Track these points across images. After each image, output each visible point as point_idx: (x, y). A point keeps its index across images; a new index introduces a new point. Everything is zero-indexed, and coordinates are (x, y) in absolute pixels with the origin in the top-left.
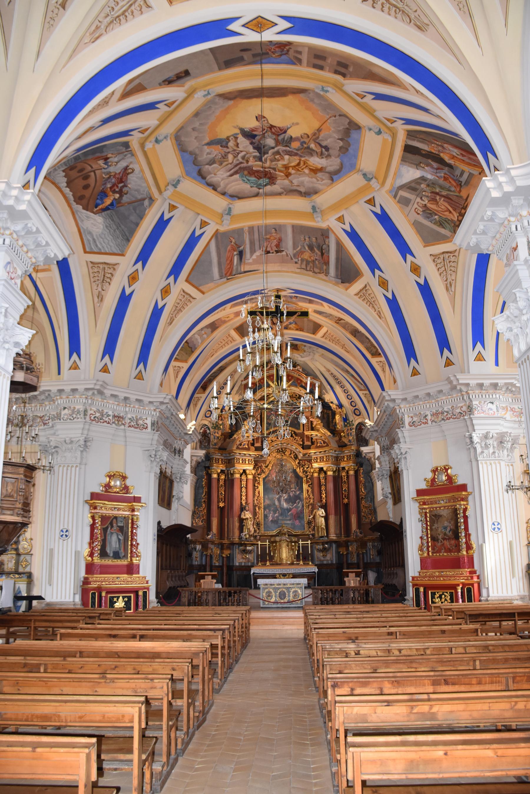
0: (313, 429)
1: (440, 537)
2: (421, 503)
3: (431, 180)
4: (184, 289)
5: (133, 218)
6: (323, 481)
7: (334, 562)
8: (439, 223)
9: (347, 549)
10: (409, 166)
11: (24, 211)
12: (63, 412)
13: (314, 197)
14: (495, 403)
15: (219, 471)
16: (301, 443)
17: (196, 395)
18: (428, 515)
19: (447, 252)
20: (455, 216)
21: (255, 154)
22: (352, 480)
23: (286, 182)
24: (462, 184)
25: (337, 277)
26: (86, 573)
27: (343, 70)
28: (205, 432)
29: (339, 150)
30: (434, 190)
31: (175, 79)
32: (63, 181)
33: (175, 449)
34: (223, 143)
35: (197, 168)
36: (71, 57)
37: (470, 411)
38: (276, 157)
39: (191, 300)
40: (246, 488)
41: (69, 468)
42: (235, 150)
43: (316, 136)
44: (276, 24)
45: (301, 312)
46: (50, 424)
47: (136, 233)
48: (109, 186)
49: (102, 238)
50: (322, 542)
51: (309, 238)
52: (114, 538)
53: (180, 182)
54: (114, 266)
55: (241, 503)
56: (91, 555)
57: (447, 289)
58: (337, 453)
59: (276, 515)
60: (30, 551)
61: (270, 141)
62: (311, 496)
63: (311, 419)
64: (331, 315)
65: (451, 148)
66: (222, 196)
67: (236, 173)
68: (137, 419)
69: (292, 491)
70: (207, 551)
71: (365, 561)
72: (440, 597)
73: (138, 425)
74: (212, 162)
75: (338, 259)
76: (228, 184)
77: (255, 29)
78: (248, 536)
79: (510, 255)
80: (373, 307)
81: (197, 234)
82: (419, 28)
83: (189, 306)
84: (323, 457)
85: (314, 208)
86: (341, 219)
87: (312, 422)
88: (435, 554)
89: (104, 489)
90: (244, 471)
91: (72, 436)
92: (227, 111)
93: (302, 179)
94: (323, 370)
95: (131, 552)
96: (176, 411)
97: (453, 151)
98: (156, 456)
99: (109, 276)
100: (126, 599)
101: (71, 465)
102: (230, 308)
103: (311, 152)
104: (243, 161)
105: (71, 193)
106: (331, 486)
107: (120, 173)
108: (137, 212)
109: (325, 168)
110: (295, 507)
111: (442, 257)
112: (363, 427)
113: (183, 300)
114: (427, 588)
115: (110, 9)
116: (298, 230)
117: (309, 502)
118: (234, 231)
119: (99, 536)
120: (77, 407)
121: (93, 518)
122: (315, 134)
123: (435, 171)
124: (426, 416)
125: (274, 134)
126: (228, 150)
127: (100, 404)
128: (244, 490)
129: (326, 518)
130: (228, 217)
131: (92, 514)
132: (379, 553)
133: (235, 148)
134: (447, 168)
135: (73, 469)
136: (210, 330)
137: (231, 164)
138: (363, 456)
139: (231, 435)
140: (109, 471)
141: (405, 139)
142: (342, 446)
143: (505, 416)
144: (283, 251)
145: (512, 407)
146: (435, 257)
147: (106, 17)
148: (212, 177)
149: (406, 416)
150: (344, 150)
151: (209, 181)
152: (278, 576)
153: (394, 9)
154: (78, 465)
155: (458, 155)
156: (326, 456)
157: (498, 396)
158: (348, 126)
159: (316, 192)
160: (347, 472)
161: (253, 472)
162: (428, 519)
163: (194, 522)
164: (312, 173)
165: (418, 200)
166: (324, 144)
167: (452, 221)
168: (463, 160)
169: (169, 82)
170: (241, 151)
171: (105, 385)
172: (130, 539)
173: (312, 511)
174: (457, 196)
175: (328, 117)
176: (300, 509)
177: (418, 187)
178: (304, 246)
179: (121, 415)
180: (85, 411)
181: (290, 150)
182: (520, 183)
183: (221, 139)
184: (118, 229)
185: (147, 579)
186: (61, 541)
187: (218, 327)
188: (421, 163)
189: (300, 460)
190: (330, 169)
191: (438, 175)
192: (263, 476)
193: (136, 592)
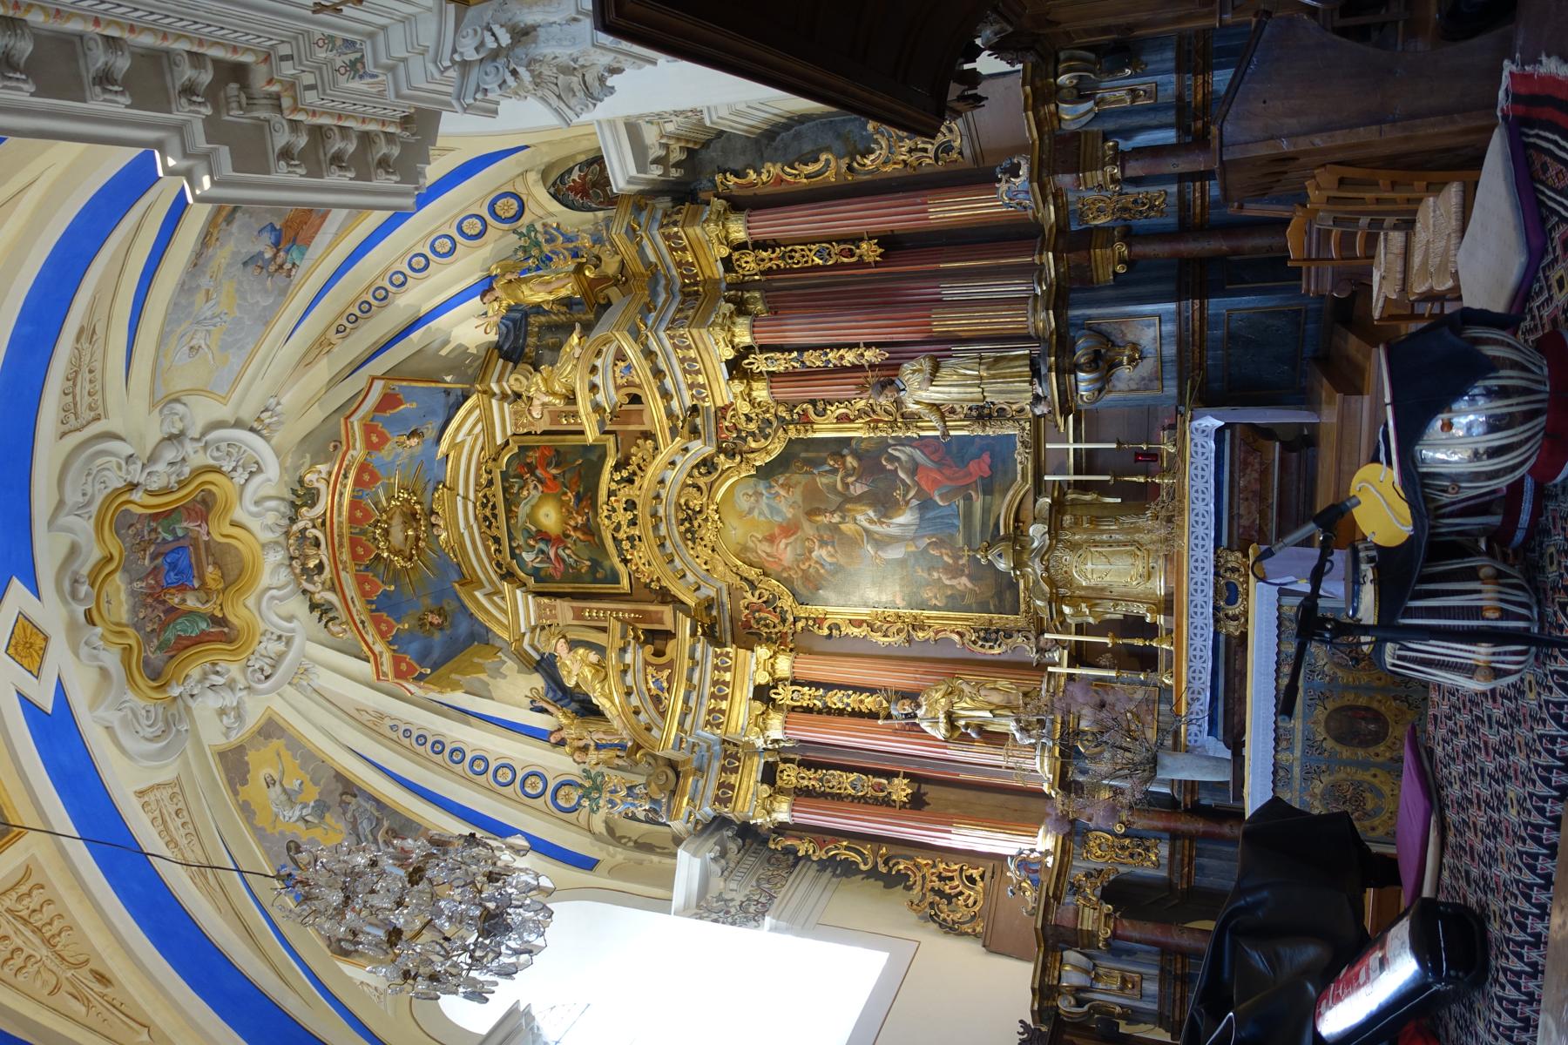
7: (1172, 306)
15: (765, 790)
22: (772, 225)
40: (829, 687)
50: (1060, 372)
59: (946, 558)
69: (846, 486)
71: (1169, 136)
84: (682, 360)
90: (762, 694)
94: (323, 370)
112: (575, 175)
128: (836, 699)
138: (675, 173)
152: (1232, 628)
160: (741, 246)
176: (918, 454)
189: (720, 450)
192: (787, 602)
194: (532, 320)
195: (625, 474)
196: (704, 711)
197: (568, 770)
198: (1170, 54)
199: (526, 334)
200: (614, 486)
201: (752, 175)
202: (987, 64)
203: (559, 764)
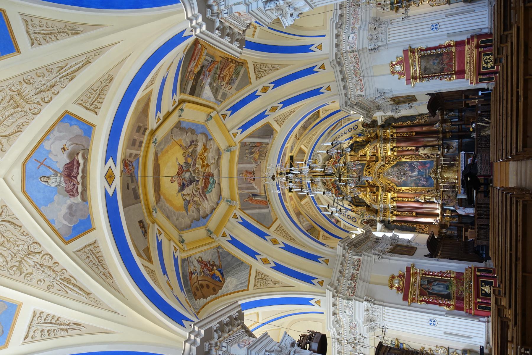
0: (365, 155)
1: (441, 66)
2: (416, 81)
3: (211, 80)
4: (274, 230)
5: (229, 259)
6: (400, 149)
7: (458, 141)
8: (237, 75)
9: (448, 132)
10: (203, 93)
11: (205, 331)
12: (348, 313)
13: (221, 150)
14: (348, 35)
16: (374, 162)
17: (342, 227)
18: (424, 76)
19: (255, 70)
20: (233, 65)
21: (194, 185)
23: (212, 166)
24: (213, 60)
25: (269, 138)
26: (463, 310)
27: (142, 129)
28: (365, 222)
29: (193, 134)
30: (217, 78)
31: (144, 229)
32: (203, 301)
33: (376, 242)
34: (187, 203)
35: (202, 219)
36: (119, 292)
37: (354, 51)
38: (197, 172)
39: (280, 226)
40: (403, 198)
41: (385, 313)
42: (192, 196)
43: (185, 148)
44: (110, 167)
45: (290, 160)
46: (356, 323)
47: (238, 258)
48: (208, 272)
49: (240, 279)
51: (246, 154)
52: (436, 288)
53: (209, 229)
54: (257, 273)
55: (413, 201)
56: (449, 306)
57: (277, 69)
58: (381, 140)
60: (446, 348)
61: (187, 175)
62: (410, 156)
63: (359, 156)
64: (293, 142)
65: (191, 67)
66: (219, 205)
67: (205, 196)
68: (354, 265)
70: (447, 225)
71: (457, 120)
72: (486, 63)
73: (358, 265)
74: (198, 210)
75: (259, 137)
76: (212, 201)
77: (112, 180)
78: (437, 198)
79: (244, 17)
80: (288, 116)
81: (241, 221)
82: (111, 80)
83: (284, 228)
85: (228, 151)
86: (235, 135)
87: (361, 156)
88: (454, 70)
89: (401, 292)
91: (364, 310)
92: (167, 200)
93: (210, 158)
95: (446, 277)
96: (350, 240)
97: (193, 65)
98: (378, 255)
99: (263, 276)
100: (483, 284)
101: (384, 312)
102: (287, 203)
103: (194, 151)
104: (198, 192)
105: (211, 296)
106: (403, 144)
107: (201, 265)
108: (225, 256)
109: (204, 143)
110: (417, 166)
111: (257, 73)
113: (280, 232)
114: (480, 74)
115: (94, 266)
116: (241, 160)
117: (414, 158)
118: (240, 199)
119: (434, 299)
120: (345, 304)
121: (421, 301)
122: (183, 149)
123: (205, 77)
124: (356, 81)
125: (182, 173)
126: (192, 200)
127: (343, 289)
128: (404, 199)
129: (425, 146)
130: (232, 201)
131: (418, 301)
132: (452, 110)
133: (190, 196)
134: (203, 70)
135: (386, 311)
136: (301, 216)
137: (200, 199)
138: (384, 123)
139: (368, 206)
140: (388, 287)
141: (186, 95)
142: (377, 137)
143: (357, 27)
144: (253, 170)
145: (352, 24)
146: (257, 78)
147: (98, 268)
148: (207, 210)
149: (356, 94)
150: (193, 132)
151: (210, 213)
153: (100, 95)
154: (383, 307)
155: (195, 62)
156: (383, 146)
157: (344, 34)
158: (179, 129)
159: (218, 149)
161: (392, 193)
162: (427, 76)
163: (426, 233)
164: (207, 151)
165: (223, 87)
166: (189, 143)
167: (235, 67)
168: (198, 59)
169: (145, 233)
170: (192, 192)
171: (331, 284)
172: (437, 277)
173: (420, 156)
174: (220, 64)
175: (172, 140)
176: (418, 164)
177: (215, 88)
178: (251, 157)
179: (351, 275)
180: (347, 299)
181: (192, 163)
182: (196, 11)
183: (184, 204)
184: (235, 269)
185: (467, 268)
186: (438, 326)
187: (299, 211)
188: (200, 86)
189: (385, 163)
190: (205, 141)
191: (208, 75)
192: (395, 187)
193: (477, 277)
194: (355, 144)
195: (369, 167)
196: (382, 202)
197: (353, 215)
198: (457, 111)
199: (353, 146)
200: (367, 169)
201: (397, 124)
202: (437, 111)
203: (353, 214)
